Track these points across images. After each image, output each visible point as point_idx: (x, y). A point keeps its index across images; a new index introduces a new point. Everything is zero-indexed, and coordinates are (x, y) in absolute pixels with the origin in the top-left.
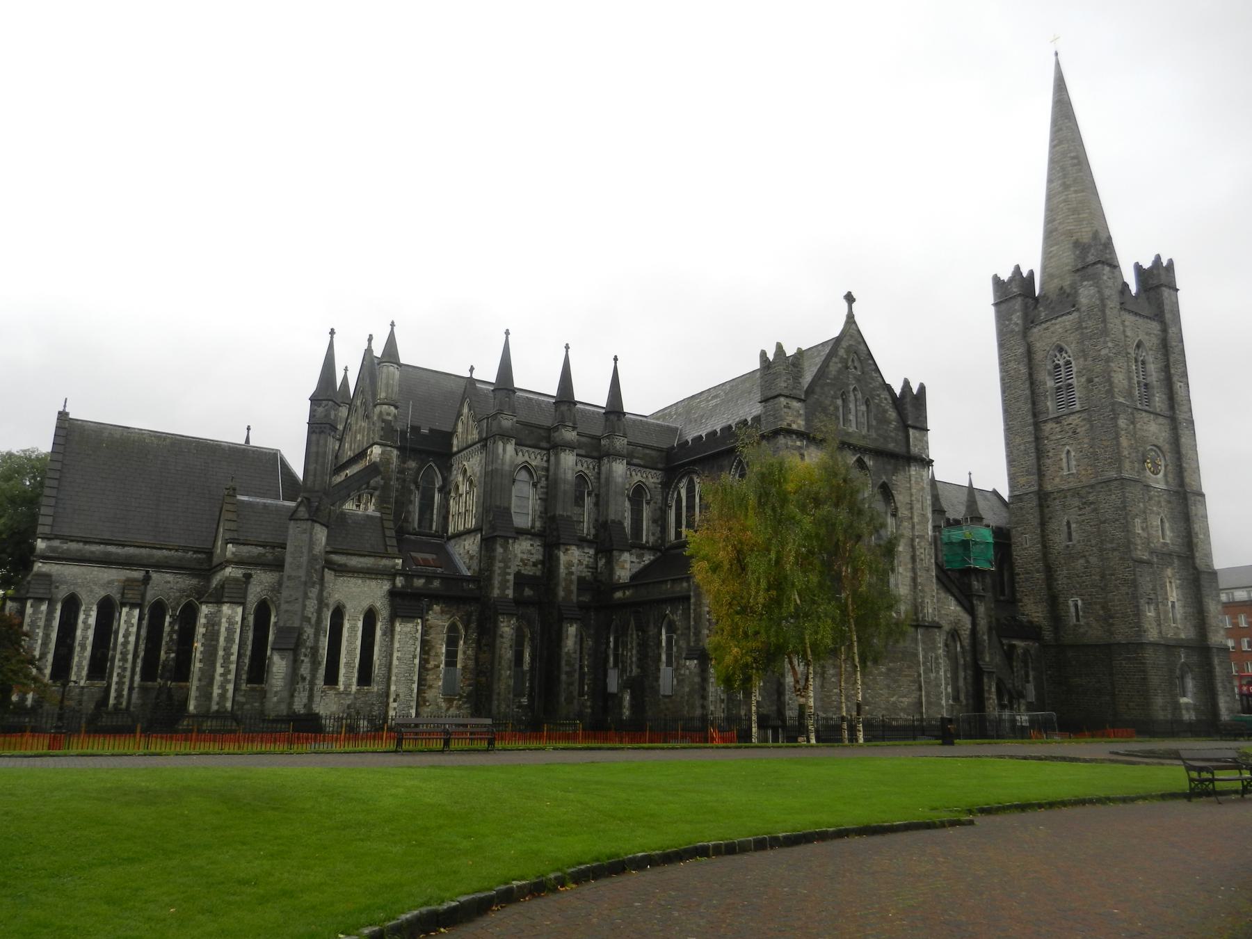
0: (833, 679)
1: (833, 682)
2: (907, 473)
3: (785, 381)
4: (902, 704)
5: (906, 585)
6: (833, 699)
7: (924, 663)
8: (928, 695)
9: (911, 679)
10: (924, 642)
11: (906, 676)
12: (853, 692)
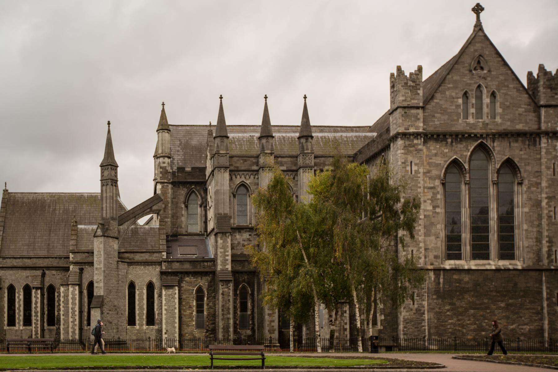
0: (448, 313)
1: (448, 315)
2: (538, 146)
3: (403, 96)
4: (522, 331)
5: (532, 238)
6: (449, 327)
7: (548, 299)
8: (551, 323)
9: (534, 311)
10: (547, 282)
11: (527, 309)
12: (469, 322)
